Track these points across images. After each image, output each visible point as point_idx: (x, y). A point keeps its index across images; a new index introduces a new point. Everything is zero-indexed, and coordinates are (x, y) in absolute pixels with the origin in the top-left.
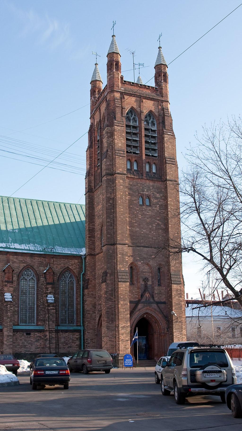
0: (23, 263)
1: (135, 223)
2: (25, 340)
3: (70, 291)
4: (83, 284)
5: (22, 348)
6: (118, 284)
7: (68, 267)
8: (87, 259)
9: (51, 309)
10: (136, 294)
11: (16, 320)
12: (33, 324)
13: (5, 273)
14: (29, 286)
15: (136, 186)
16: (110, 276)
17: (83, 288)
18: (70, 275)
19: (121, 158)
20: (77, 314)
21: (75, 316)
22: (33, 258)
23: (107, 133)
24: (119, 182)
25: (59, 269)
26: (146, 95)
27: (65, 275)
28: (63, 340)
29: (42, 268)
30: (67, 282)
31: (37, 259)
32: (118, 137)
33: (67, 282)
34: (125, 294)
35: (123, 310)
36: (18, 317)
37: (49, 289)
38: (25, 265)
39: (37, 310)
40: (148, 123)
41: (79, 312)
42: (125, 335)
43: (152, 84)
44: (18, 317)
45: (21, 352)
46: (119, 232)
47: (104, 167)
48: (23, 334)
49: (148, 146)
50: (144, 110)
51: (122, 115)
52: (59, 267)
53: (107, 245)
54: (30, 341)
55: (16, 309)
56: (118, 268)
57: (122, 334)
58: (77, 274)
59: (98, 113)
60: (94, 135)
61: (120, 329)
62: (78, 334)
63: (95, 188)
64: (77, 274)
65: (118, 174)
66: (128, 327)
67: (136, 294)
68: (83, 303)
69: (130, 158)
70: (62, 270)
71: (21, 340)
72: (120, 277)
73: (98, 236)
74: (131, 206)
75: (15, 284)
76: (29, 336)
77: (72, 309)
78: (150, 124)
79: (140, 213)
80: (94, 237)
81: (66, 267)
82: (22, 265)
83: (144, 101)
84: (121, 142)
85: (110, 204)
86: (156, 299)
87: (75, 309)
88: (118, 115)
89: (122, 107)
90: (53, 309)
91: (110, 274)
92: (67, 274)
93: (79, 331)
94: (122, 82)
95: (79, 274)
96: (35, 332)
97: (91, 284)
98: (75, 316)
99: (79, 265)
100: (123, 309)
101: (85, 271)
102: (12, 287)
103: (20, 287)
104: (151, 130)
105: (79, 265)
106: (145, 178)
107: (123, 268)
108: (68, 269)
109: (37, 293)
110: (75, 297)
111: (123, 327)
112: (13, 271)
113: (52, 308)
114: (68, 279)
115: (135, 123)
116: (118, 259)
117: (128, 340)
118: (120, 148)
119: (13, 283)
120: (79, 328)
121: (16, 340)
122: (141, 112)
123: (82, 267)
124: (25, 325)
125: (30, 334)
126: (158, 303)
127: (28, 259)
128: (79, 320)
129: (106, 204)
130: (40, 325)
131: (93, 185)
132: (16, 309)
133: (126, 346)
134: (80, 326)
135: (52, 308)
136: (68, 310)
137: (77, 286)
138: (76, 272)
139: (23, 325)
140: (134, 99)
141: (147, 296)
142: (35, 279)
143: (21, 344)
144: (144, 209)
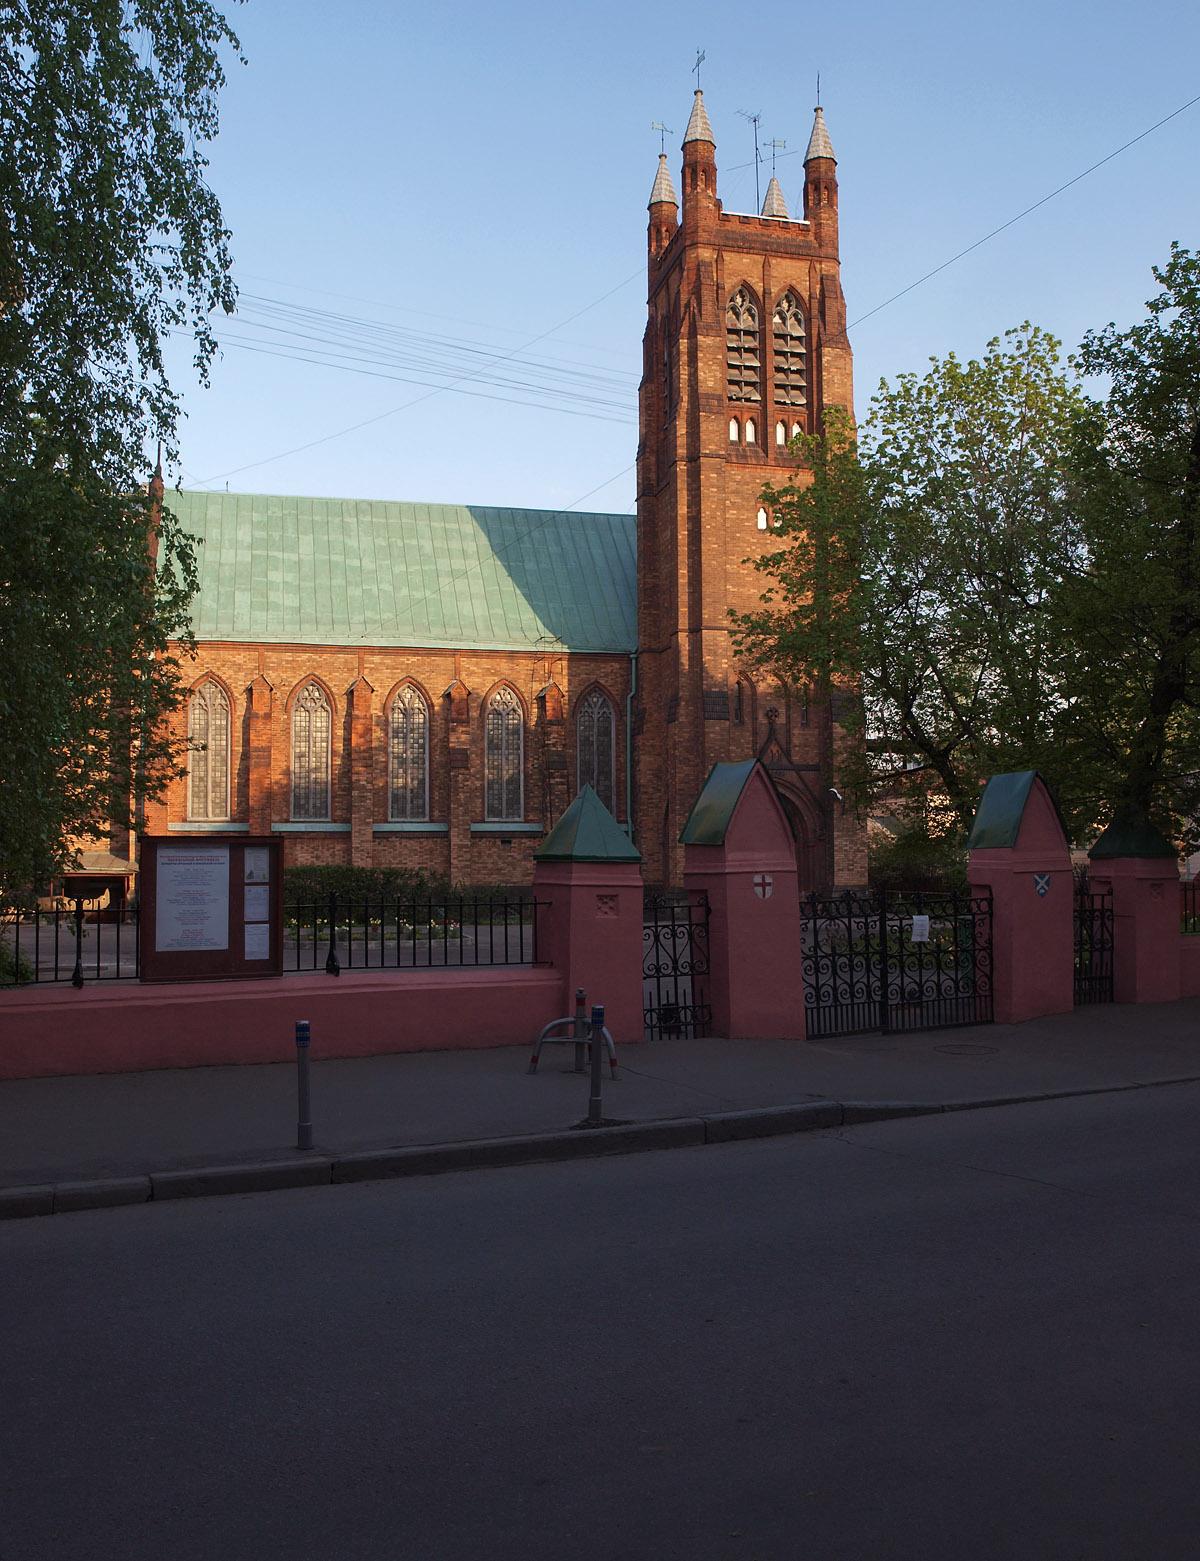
2: (499, 857)
3: (601, 739)
4: (631, 722)
5: (492, 874)
9: (557, 784)
10: (747, 748)
11: (478, 811)
12: (517, 819)
14: (507, 729)
15: (751, 485)
17: (632, 730)
18: (601, 700)
20: (618, 795)
21: (614, 797)
22: (516, 661)
25: (575, 687)
27: (590, 699)
30: (595, 717)
31: (525, 665)
32: (706, 363)
33: (595, 717)
36: (483, 803)
37: (552, 736)
38: (497, 679)
39: (526, 786)
41: (622, 788)
43: (795, 214)
44: (483, 803)
45: (491, 883)
48: (495, 843)
49: (784, 380)
50: (774, 286)
54: (510, 858)
55: (478, 784)
56: (704, 687)
58: (617, 698)
59: (663, 293)
60: (657, 348)
63: (658, 485)
64: (617, 698)
65: (706, 456)
67: (747, 748)
68: (632, 766)
69: (738, 415)
70: (583, 688)
71: (489, 856)
73: (666, 605)
74: (738, 535)
75: (474, 725)
76: (507, 846)
77: (607, 783)
78: (789, 323)
79: (759, 550)
81: (592, 681)
82: (490, 681)
83: (774, 261)
84: (715, 376)
86: (795, 758)
87: (613, 784)
90: (562, 784)
91: (687, 702)
95: (624, 697)
96: (522, 838)
97: (651, 722)
98: (614, 797)
99: (622, 676)
102: (467, 733)
103: (486, 731)
104: (791, 337)
105: (622, 676)
106: (773, 463)
109: (525, 746)
110: (613, 754)
113: (558, 780)
114: (596, 710)
118: (710, 391)
119: (468, 722)
121: (480, 856)
123: (629, 681)
124: (499, 822)
125: (510, 842)
126: (798, 769)
127: (504, 666)
128: (623, 808)
130: (532, 821)
132: (478, 784)
135: (558, 780)
137: (617, 726)
139: (494, 822)
140: (746, 259)
143: (490, 866)
144: (769, 542)
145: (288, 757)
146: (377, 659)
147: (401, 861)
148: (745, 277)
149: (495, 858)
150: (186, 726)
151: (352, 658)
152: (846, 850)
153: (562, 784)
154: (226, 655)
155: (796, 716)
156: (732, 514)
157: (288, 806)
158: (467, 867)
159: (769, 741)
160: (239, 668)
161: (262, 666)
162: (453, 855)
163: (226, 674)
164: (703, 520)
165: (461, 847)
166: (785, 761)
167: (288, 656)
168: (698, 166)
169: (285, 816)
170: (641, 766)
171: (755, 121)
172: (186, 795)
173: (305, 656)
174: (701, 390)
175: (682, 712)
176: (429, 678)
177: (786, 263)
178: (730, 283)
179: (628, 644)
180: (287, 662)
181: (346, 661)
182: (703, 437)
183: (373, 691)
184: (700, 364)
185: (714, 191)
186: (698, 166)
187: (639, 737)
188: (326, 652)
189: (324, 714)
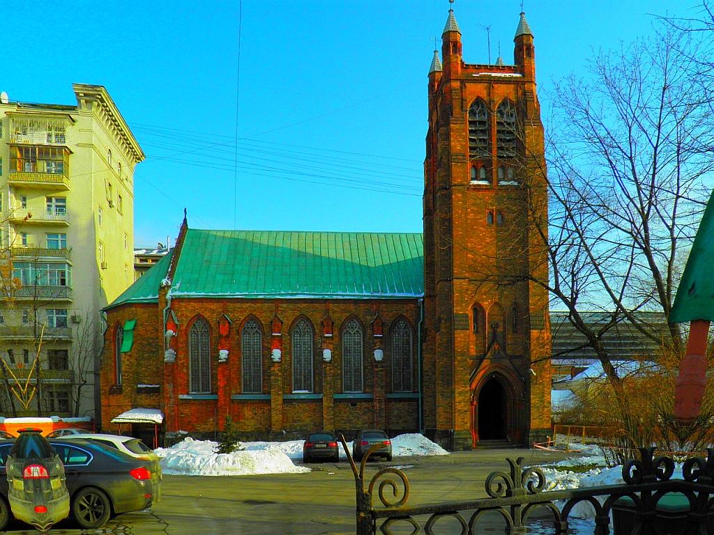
0: (347, 312)
1: (481, 249)
7: (402, 315)
11: (339, 387)
13: (324, 326)
16: (445, 323)
17: (421, 341)
19: (459, 164)
23: (441, 135)
24: (457, 197)
28: (396, 412)
29: (369, 318)
31: (362, 307)
36: (342, 382)
38: (348, 314)
40: (502, 114)
42: (463, 404)
46: (456, 262)
52: (391, 315)
55: (339, 372)
57: (460, 402)
61: (457, 395)
62: (416, 403)
64: (413, 323)
65: (455, 185)
66: (467, 392)
69: (475, 164)
71: (345, 412)
72: (456, 323)
76: (354, 407)
77: (408, 370)
82: (345, 315)
86: (509, 352)
87: (411, 370)
88: (457, 110)
90: (382, 371)
92: (402, 324)
93: (417, 400)
94: (462, 67)
95: (417, 323)
98: (412, 379)
100: (461, 367)
101: (423, 318)
107: (461, 310)
108: (402, 317)
109: (364, 351)
111: (460, 393)
112: (333, 323)
115: (483, 117)
116: (455, 299)
117: (466, 411)
120: (415, 396)
121: (340, 413)
122: (491, 101)
125: (356, 405)
126: (511, 358)
127: (352, 307)
130: (368, 392)
131: (431, 205)
132: (339, 372)
133: (464, 419)
134: (418, 392)
136: (403, 371)
141: (496, 348)
142: (361, 332)
145: (240, 358)
146: (285, 305)
147: (298, 416)
149: (348, 413)
150: (187, 343)
151: (272, 306)
153: (382, 371)
154: (206, 305)
155: (509, 328)
156: (471, 216)
157: (240, 385)
158: (331, 419)
159: (493, 341)
160: (214, 311)
161: (225, 311)
162: (325, 412)
163: (207, 315)
164: (454, 219)
165: (328, 408)
166: (502, 353)
167: (238, 305)
168: (450, 44)
169: (239, 391)
171: (488, 29)
172: (188, 380)
173: (247, 305)
174: (453, 152)
175: (442, 326)
176: (312, 315)
180: (239, 308)
181: (269, 307)
182: (454, 175)
183: (282, 323)
184: (452, 138)
186: (450, 44)
188: (258, 303)
189: (258, 335)
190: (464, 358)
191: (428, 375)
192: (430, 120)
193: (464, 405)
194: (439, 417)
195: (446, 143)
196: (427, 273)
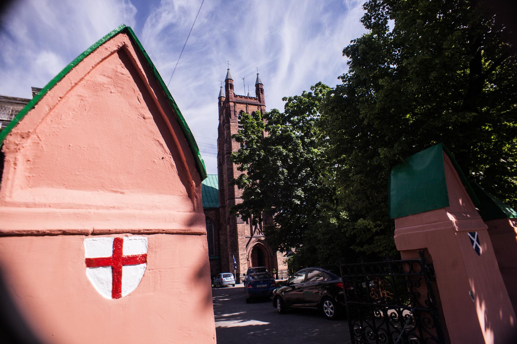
6: (237, 225)
8: (220, 209)
23: (226, 127)
26: (250, 102)
32: (233, 129)
34: (242, 231)
35: (241, 243)
47: (225, 149)
51: (235, 116)
53: (228, 199)
57: (242, 259)
59: (222, 116)
61: (240, 256)
66: (245, 254)
72: (238, 220)
80: (224, 195)
85: (229, 172)
87: (214, 245)
89: (235, 111)
94: (234, 96)
100: (241, 242)
111: (242, 255)
117: (245, 264)
129: (227, 172)
133: (244, 267)
138: (213, 219)
140: (242, 105)
148: (242, 109)
152: (281, 259)
164: (234, 168)
168: (229, 85)
170: (221, 239)
175: (231, 222)
177: (252, 106)
178: (238, 111)
179: (218, 206)
184: (231, 129)
185: (233, 90)
186: (229, 85)
187: (220, 231)
190: (242, 237)
191: (223, 247)
192: (220, 119)
193: (244, 261)
194: (231, 268)
195: (228, 131)
196: (221, 195)
